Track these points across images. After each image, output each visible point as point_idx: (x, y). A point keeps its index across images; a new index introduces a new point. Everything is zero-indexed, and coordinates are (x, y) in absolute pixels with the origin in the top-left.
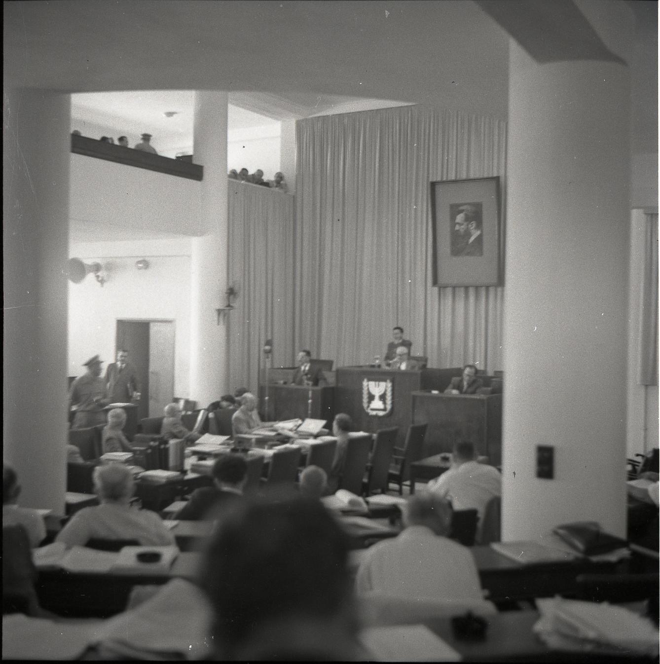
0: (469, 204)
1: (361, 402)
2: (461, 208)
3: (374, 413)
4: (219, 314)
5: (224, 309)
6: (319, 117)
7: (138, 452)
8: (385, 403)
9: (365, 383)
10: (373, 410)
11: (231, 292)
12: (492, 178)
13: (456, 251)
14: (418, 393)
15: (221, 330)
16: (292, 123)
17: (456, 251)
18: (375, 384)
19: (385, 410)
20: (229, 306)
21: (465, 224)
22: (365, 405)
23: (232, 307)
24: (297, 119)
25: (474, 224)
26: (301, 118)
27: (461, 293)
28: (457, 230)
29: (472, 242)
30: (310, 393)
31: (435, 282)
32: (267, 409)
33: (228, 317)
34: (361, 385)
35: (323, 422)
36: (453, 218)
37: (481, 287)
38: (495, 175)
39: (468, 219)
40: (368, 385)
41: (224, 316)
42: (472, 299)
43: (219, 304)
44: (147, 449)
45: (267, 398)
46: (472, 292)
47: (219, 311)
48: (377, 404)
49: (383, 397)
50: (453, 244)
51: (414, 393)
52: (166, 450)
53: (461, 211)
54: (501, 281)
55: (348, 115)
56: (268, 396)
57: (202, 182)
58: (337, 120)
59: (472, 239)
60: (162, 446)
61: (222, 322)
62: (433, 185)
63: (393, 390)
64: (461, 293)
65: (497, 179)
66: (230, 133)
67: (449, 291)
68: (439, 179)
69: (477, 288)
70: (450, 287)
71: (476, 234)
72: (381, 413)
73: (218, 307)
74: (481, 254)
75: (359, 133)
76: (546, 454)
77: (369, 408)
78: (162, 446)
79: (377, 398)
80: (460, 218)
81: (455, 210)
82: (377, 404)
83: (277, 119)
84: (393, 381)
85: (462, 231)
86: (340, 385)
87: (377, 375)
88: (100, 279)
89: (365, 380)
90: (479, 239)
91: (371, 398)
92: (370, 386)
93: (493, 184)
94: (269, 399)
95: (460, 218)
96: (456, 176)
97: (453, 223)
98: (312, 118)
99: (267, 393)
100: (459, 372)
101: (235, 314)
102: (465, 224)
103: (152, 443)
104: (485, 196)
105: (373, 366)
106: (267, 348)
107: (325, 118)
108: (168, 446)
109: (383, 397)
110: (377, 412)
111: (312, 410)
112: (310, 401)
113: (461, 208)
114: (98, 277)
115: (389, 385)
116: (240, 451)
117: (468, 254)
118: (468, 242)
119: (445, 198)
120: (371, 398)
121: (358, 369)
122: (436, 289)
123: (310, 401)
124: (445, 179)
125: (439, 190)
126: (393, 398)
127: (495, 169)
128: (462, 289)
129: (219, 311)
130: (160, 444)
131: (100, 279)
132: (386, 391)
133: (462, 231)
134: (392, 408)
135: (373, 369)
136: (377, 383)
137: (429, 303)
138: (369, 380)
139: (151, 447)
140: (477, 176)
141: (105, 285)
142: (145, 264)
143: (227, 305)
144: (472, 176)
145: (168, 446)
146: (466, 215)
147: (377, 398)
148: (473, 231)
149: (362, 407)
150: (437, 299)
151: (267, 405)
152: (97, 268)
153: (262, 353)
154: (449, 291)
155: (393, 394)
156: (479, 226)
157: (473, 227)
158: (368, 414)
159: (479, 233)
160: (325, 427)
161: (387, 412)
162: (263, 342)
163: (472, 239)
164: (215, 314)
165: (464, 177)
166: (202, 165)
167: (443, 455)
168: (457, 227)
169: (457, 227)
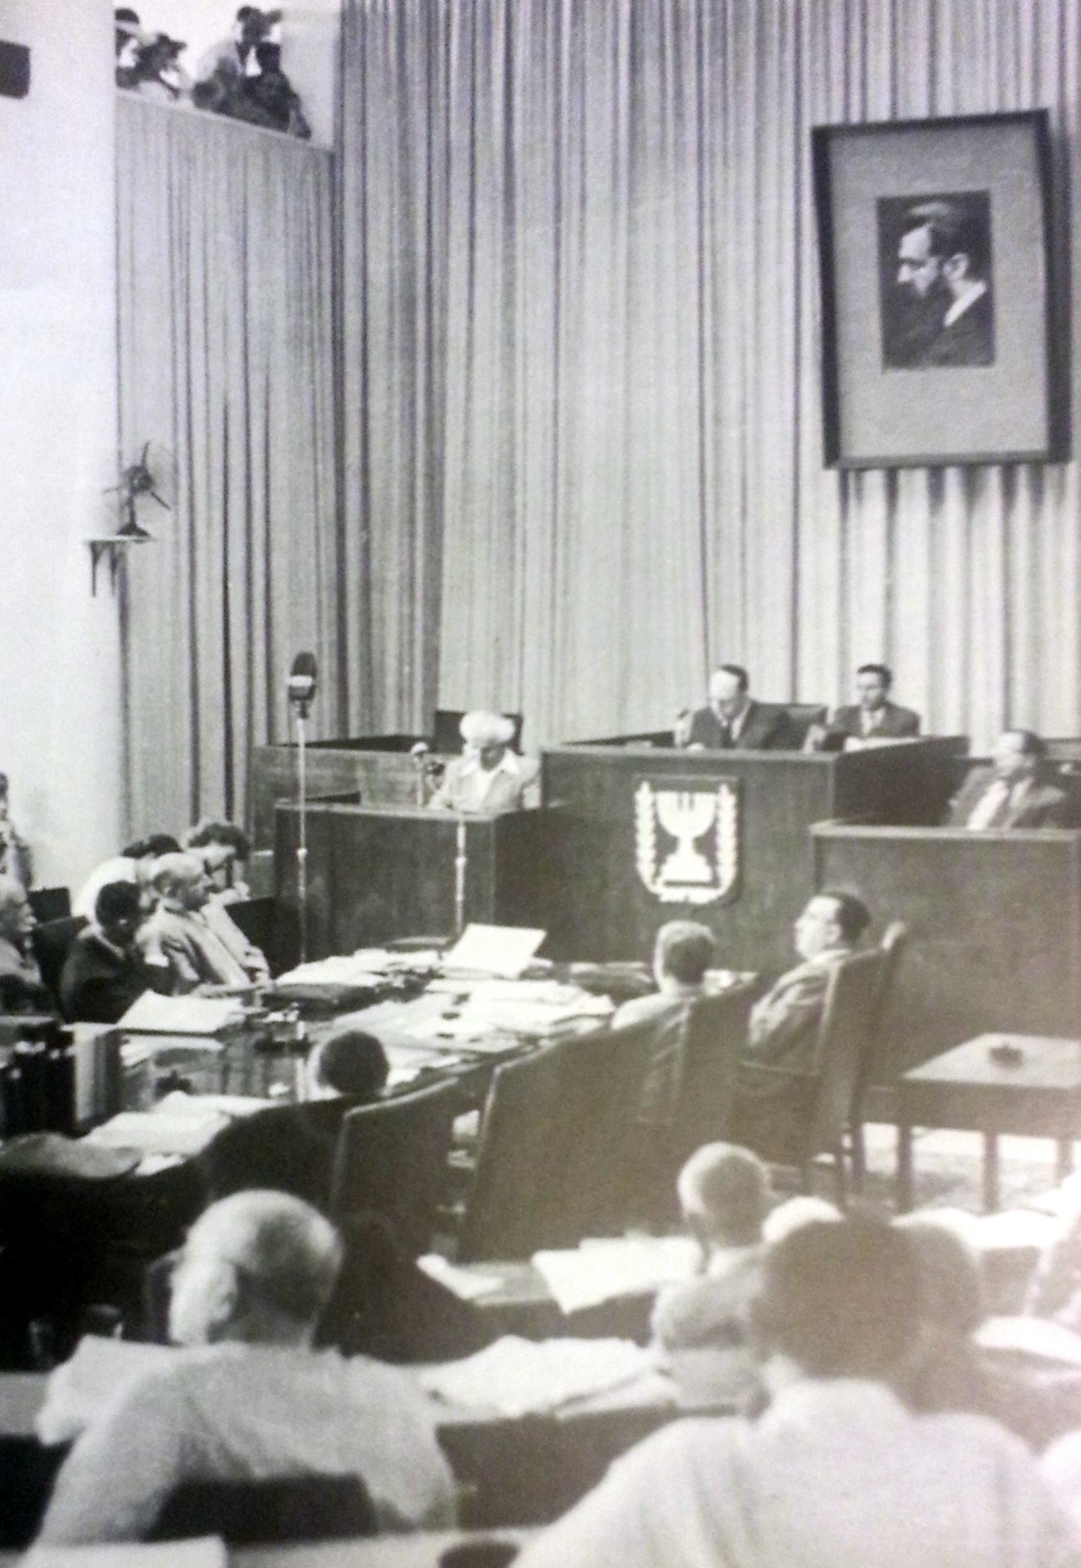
2: (921, 211)
8: (712, 861)
9: (644, 796)
10: (670, 884)
14: (825, 828)
18: (680, 802)
19: (714, 883)
21: (933, 262)
25: (962, 263)
27: (915, 483)
29: (957, 322)
30: (461, 833)
31: (833, 451)
32: (302, 889)
35: (535, 937)
38: (1026, 105)
39: (941, 247)
40: (654, 804)
49: (706, 845)
51: (825, 828)
52: (67, 1065)
53: (918, 222)
56: (308, 846)
59: (954, 314)
60: (55, 1054)
64: (915, 483)
65: (1036, 119)
70: (876, 468)
71: (967, 294)
72: (702, 896)
77: (660, 881)
78: (55, 1054)
79: (686, 846)
80: (914, 243)
84: (740, 791)
86: (554, 804)
89: (645, 787)
91: (666, 844)
95: (914, 243)
99: (303, 839)
102: (933, 262)
103: (23, 1047)
106: (303, 681)
108: (71, 1051)
109: (706, 845)
111: (466, 891)
115: (727, 801)
116: (286, 1050)
117: (945, 360)
118: (939, 327)
120: (666, 844)
122: (831, 477)
126: (740, 848)
128: (920, 478)
130: (50, 1047)
132: (716, 820)
135: (665, 752)
136: (686, 796)
138: (656, 788)
139: (19, 1060)
144: (946, 109)
145: (71, 1051)
147: (686, 846)
149: (637, 880)
151: (302, 873)
153: (282, 696)
155: (740, 833)
156: (980, 268)
160: (541, 952)
163: (954, 314)
165: (920, 111)
168: (905, 274)
169: (905, 274)
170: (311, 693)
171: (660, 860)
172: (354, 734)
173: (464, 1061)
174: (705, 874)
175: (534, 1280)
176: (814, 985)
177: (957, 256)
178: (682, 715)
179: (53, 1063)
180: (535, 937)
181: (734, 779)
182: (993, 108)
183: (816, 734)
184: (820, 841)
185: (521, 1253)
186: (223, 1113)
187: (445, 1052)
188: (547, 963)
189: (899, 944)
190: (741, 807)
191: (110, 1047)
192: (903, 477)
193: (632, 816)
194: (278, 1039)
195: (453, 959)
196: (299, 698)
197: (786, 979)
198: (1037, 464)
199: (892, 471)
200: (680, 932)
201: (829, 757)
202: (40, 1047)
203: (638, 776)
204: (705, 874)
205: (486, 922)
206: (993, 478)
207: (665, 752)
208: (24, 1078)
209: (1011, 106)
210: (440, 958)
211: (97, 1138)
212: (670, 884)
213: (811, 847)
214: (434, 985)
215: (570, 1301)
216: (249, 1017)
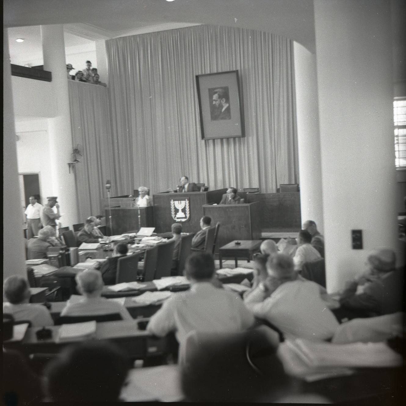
0: (221, 88)
1: (170, 214)
2: (216, 91)
3: (179, 220)
4: (70, 167)
5: (72, 163)
6: (120, 38)
7: (53, 258)
8: (185, 214)
9: (172, 202)
10: (178, 218)
11: (76, 151)
12: (233, 72)
13: (214, 117)
14: (206, 206)
15: (72, 176)
16: (103, 43)
17: (214, 117)
19: (186, 217)
21: (219, 100)
22: (173, 216)
23: (78, 161)
24: (106, 40)
25: (224, 100)
26: (108, 39)
28: (214, 105)
31: (203, 137)
33: (75, 169)
34: (170, 204)
35: (153, 229)
36: (211, 97)
37: (231, 138)
38: (234, 69)
39: (220, 97)
40: (174, 204)
41: (73, 167)
42: (225, 146)
45: (110, 217)
46: (225, 140)
48: (180, 214)
49: (184, 210)
50: (212, 113)
52: (68, 255)
53: (216, 93)
54: (243, 134)
55: (139, 35)
57: (52, 82)
58: (132, 39)
59: (223, 110)
60: (67, 253)
61: (71, 171)
62: (197, 77)
63: (190, 205)
65: (237, 72)
66: (66, 48)
67: (211, 142)
68: (200, 73)
69: (228, 139)
71: (225, 106)
72: (183, 220)
74: (230, 118)
75: (147, 46)
76: (358, 235)
77: (176, 218)
78: (67, 253)
79: (180, 211)
80: (215, 97)
81: (212, 92)
82: (180, 214)
83: (94, 41)
84: (189, 200)
85: (217, 105)
86: (156, 205)
87: (178, 196)
89: (172, 200)
90: (228, 109)
91: (177, 211)
92: (175, 203)
93: (234, 76)
94: (112, 218)
95: (215, 97)
96: (210, 71)
97: (211, 100)
98: (116, 39)
99: (110, 214)
100: (224, 191)
101: (78, 166)
103: (61, 251)
104: (231, 83)
105: (176, 191)
106: (108, 185)
107: (124, 38)
108: (69, 252)
109: (184, 210)
110: (181, 219)
111: (141, 222)
113: (216, 91)
115: (187, 202)
117: (222, 118)
118: (221, 112)
119: (205, 85)
120: (177, 211)
121: (167, 194)
122: (203, 141)
123: (139, 216)
124: (203, 73)
125: (201, 80)
126: (190, 211)
127: (234, 66)
128: (219, 141)
132: (185, 206)
133: (217, 105)
134: (190, 216)
136: (180, 201)
137: (200, 152)
138: (174, 201)
139: (61, 254)
140: (224, 70)
144: (220, 71)
145: (69, 252)
146: (219, 95)
147: (180, 211)
148: (224, 105)
149: (172, 217)
150: (204, 148)
151: (111, 221)
153: (105, 188)
154: (211, 142)
155: (190, 208)
156: (228, 101)
157: (224, 101)
159: (227, 105)
160: (154, 232)
161: (187, 219)
162: (105, 181)
163: (223, 110)
164: (67, 167)
165: (215, 71)
166: (50, 71)
167: (236, 241)
169: (214, 103)
171: (176, 214)
172: (119, 195)
173: (141, 251)
174: (184, 216)
175: (154, 285)
176: (204, 233)
177: (223, 99)
179: (66, 255)
180: (153, 229)
181: (188, 198)
182: (228, 70)
183: (203, 188)
184: (204, 208)
185: (151, 280)
186: (97, 262)
187: (137, 249)
188: (155, 233)
189: (219, 226)
190: (189, 203)
191: (77, 251)
192: (216, 140)
193: (170, 206)
194: (107, 249)
195: (139, 234)
196: (107, 188)
197: (199, 232)
198: (239, 137)
199: (214, 140)
201: (205, 192)
202: (64, 251)
203: (170, 198)
204: (184, 216)
205: (145, 227)
206: (232, 140)
207: (176, 193)
208: (61, 258)
209: (231, 70)
210: (136, 234)
211: (75, 267)
212: (178, 218)
213: (203, 208)
214: (136, 239)
215: (159, 288)
216: (102, 246)
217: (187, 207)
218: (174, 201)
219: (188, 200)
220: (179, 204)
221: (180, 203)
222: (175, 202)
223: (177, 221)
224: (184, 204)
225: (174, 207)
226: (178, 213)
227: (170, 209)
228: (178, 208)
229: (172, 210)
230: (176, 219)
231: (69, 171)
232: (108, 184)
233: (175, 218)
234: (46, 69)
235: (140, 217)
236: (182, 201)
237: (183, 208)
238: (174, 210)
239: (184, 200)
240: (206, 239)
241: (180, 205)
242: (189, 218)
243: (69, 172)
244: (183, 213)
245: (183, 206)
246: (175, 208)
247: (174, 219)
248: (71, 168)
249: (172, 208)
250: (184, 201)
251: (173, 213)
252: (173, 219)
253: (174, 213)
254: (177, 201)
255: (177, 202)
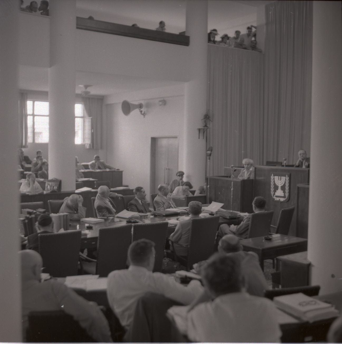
1: (270, 190)
3: (278, 199)
8: (284, 192)
9: (272, 177)
10: (277, 197)
11: (207, 117)
15: (202, 142)
19: (284, 197)
20: (206, 126)
22: (272, 193)
34: (270, 178)
35: (222, 205)
43: (200, 126)
44: (24, 220)
47: (199, 130)
48: (279, 193)
49: (283, 188)
56: (209, 185)
57: (190, 46)
72: (282, 200)
73: (200, 128)
77: (275, 195)
79: (280, 188)
82: (279, 193)
86: (257, 178)
88: (143, 113)
89: (272, 175)
91: (276, 188)
106: (209, 152)
109: (283, 188)
110: (280, 198)
112: (232, 189)
114: (141, 112)
115: (288, 178)
120: (276, 188)
123: (232, 189)
126: (290, 189)
129: (199, 130)
131: (143, 113)
132: (285, 182)
136: (280, 177)
138: (274, 176)
139: (27, 218)
141: (146, 116)
142: (164, 102)
143: (204, 125)
147: (280, 188)
149: (270, 194)
152: (140, 106)
158: (274, 199)
161: (286, 199)
164: (197, 132)
170: (210, 155)
171: (275, 191)
174: (282, 194)
178: (285, 160)
180: (222, 205)
181: (289, 174)
184: (298, 188)
200: (192, 203)
204: (282, 194)
217: (287, 185)
218: (274, 176)
219: (288, 176)
220: (279, 179)
221: (280, 179)
222: (275, 177)
223: (275, 200)
224: (284, 180)
225: (273, 183)
226: (277, 191)
227: (270, 185)
228: (277, 184)
229: (271, 186)
230: (275, 198)
231: (198, 135)
232: (209, 151)
233: (274, 196)
234: (187, 34)
235: (233, 190)
236: (282, 177)
237: (282, 185)
238: (273, 186)
239: (284, 176)
240: (250, 227)
241: (279, 181)
242: (287, 198)
243: (198, 138)
244: (282, 191)
245: (282, 183)
246: (275, 184)
247: (273, 197)
248: (201, 134)
249: (272, 183)
250: (284, 177)
251: (272, 190)
252: (272, 196)
253: (273, 189)
254: (277, 176)
255: (278, 177)
